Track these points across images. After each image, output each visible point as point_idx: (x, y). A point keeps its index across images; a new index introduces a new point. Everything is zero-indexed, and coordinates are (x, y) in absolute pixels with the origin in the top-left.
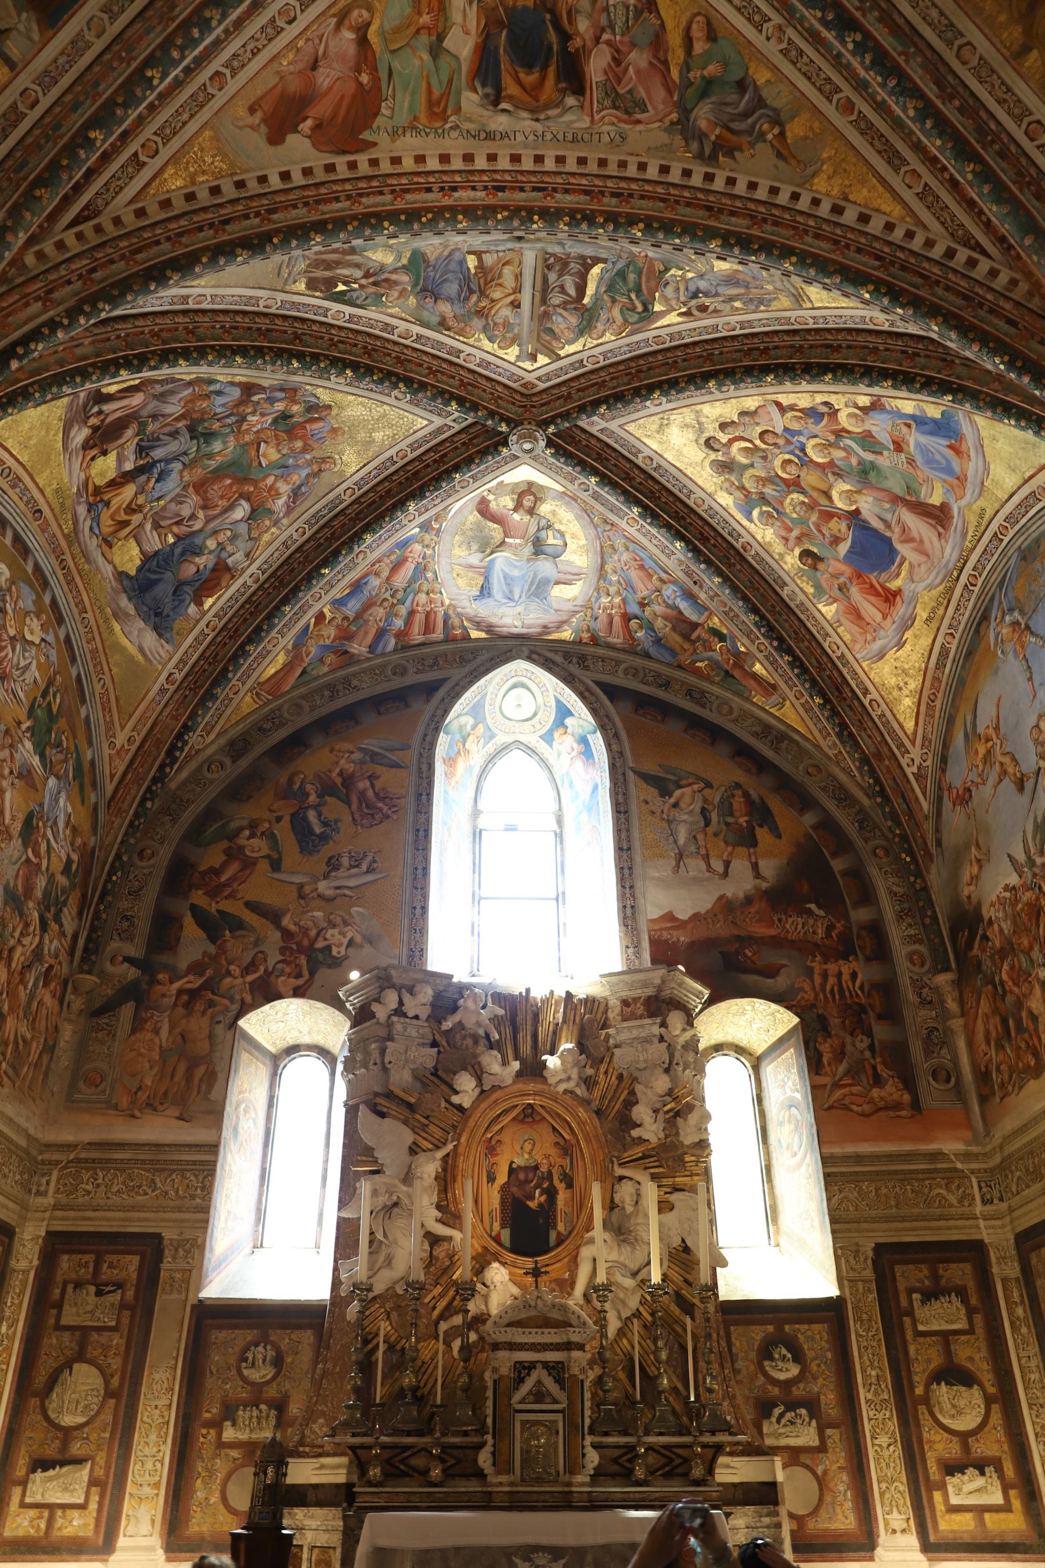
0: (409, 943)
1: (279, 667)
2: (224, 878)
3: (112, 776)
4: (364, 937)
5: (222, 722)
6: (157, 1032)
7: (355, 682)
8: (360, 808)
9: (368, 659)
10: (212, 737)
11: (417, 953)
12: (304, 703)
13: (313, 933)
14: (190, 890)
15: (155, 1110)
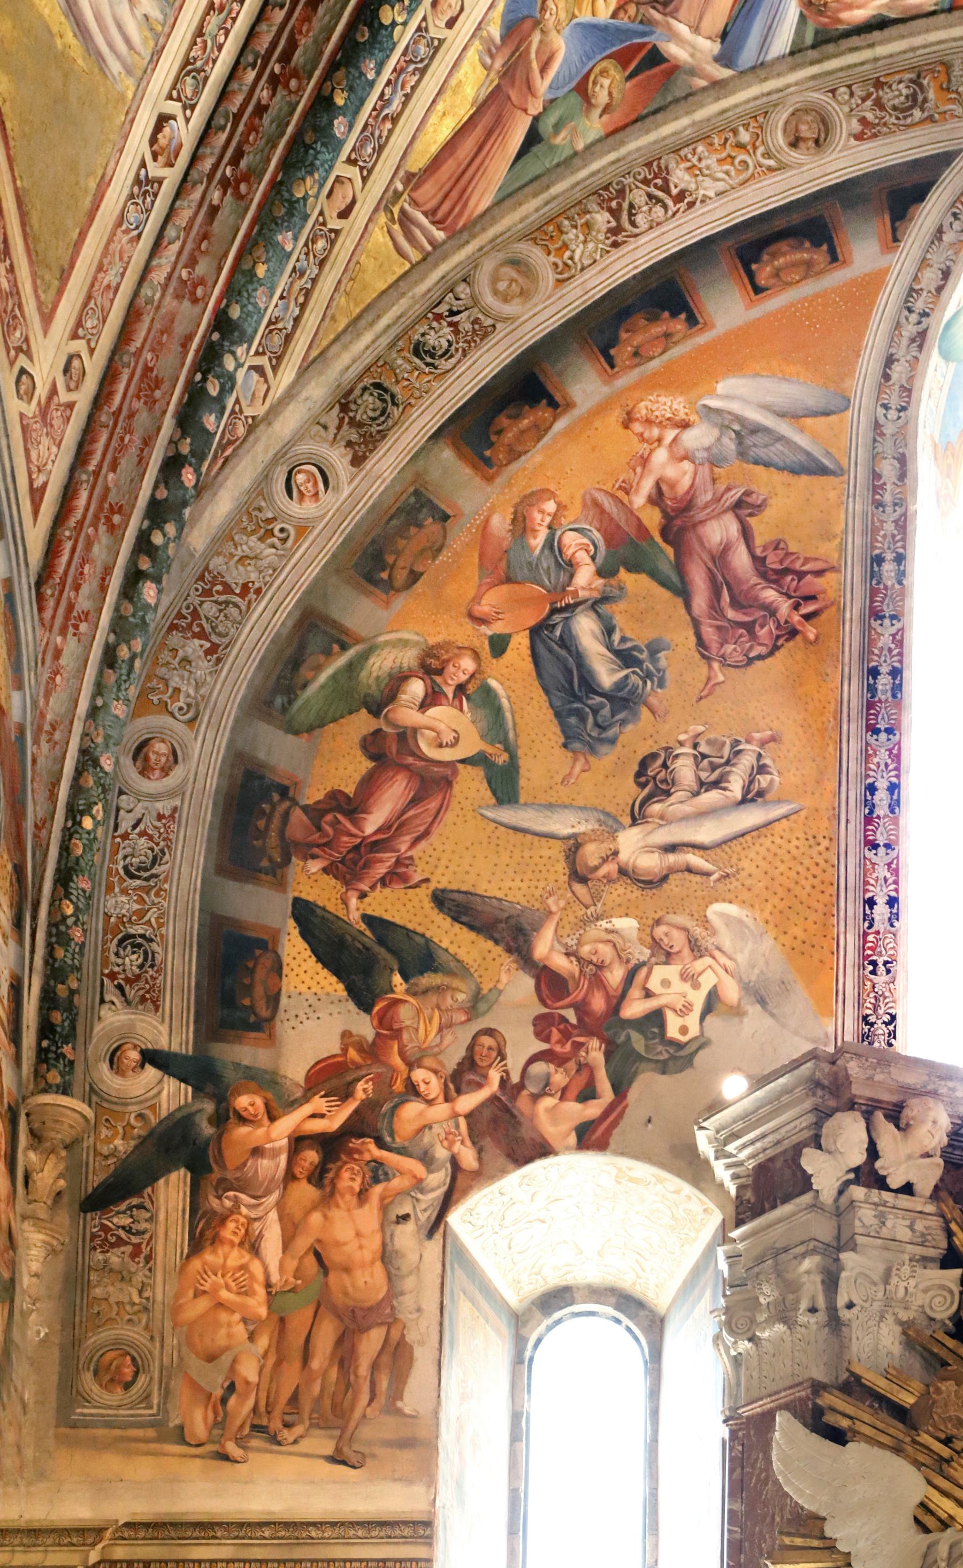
0: (860, 1003)
1: (464, 111)
2: (372, 823)
3: (37, 495)
4: (748, 988)
5: (311, 319)
6: (253, 1246)
7: (680, 177)
8: (715, 607)
9: (718, 86)
10: (287, 375)
11: (881, 1029)
12: (536, 255)
13: (615, 976)
14: (287, 861)
15: (275, 1440)
